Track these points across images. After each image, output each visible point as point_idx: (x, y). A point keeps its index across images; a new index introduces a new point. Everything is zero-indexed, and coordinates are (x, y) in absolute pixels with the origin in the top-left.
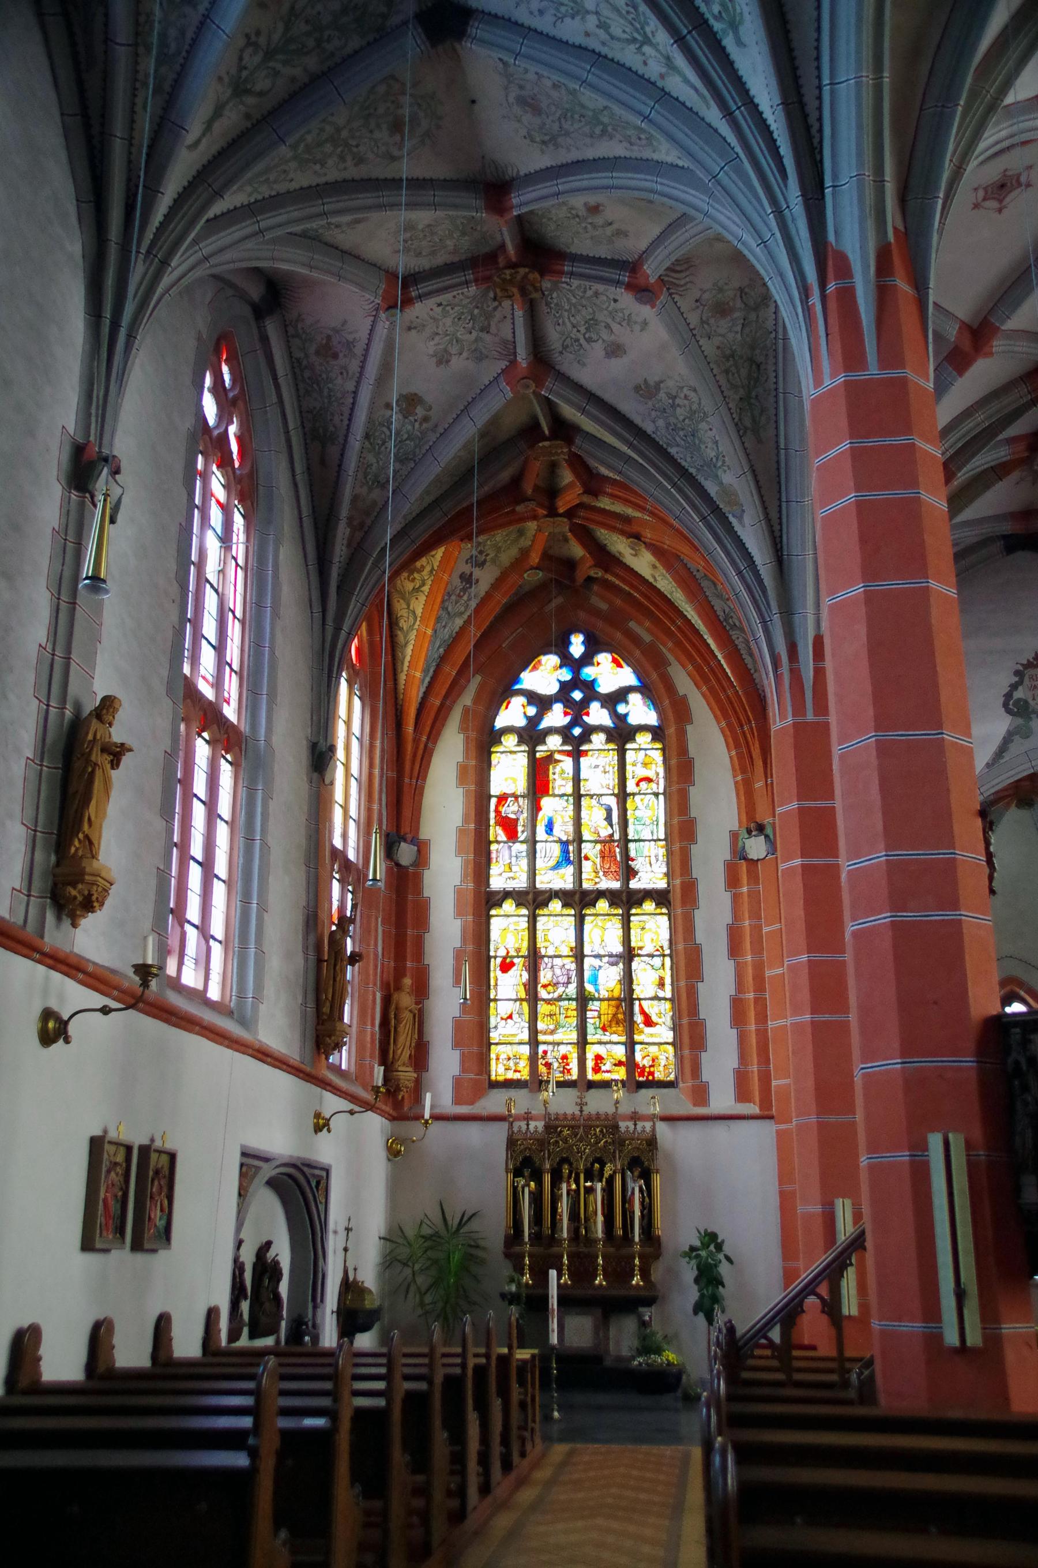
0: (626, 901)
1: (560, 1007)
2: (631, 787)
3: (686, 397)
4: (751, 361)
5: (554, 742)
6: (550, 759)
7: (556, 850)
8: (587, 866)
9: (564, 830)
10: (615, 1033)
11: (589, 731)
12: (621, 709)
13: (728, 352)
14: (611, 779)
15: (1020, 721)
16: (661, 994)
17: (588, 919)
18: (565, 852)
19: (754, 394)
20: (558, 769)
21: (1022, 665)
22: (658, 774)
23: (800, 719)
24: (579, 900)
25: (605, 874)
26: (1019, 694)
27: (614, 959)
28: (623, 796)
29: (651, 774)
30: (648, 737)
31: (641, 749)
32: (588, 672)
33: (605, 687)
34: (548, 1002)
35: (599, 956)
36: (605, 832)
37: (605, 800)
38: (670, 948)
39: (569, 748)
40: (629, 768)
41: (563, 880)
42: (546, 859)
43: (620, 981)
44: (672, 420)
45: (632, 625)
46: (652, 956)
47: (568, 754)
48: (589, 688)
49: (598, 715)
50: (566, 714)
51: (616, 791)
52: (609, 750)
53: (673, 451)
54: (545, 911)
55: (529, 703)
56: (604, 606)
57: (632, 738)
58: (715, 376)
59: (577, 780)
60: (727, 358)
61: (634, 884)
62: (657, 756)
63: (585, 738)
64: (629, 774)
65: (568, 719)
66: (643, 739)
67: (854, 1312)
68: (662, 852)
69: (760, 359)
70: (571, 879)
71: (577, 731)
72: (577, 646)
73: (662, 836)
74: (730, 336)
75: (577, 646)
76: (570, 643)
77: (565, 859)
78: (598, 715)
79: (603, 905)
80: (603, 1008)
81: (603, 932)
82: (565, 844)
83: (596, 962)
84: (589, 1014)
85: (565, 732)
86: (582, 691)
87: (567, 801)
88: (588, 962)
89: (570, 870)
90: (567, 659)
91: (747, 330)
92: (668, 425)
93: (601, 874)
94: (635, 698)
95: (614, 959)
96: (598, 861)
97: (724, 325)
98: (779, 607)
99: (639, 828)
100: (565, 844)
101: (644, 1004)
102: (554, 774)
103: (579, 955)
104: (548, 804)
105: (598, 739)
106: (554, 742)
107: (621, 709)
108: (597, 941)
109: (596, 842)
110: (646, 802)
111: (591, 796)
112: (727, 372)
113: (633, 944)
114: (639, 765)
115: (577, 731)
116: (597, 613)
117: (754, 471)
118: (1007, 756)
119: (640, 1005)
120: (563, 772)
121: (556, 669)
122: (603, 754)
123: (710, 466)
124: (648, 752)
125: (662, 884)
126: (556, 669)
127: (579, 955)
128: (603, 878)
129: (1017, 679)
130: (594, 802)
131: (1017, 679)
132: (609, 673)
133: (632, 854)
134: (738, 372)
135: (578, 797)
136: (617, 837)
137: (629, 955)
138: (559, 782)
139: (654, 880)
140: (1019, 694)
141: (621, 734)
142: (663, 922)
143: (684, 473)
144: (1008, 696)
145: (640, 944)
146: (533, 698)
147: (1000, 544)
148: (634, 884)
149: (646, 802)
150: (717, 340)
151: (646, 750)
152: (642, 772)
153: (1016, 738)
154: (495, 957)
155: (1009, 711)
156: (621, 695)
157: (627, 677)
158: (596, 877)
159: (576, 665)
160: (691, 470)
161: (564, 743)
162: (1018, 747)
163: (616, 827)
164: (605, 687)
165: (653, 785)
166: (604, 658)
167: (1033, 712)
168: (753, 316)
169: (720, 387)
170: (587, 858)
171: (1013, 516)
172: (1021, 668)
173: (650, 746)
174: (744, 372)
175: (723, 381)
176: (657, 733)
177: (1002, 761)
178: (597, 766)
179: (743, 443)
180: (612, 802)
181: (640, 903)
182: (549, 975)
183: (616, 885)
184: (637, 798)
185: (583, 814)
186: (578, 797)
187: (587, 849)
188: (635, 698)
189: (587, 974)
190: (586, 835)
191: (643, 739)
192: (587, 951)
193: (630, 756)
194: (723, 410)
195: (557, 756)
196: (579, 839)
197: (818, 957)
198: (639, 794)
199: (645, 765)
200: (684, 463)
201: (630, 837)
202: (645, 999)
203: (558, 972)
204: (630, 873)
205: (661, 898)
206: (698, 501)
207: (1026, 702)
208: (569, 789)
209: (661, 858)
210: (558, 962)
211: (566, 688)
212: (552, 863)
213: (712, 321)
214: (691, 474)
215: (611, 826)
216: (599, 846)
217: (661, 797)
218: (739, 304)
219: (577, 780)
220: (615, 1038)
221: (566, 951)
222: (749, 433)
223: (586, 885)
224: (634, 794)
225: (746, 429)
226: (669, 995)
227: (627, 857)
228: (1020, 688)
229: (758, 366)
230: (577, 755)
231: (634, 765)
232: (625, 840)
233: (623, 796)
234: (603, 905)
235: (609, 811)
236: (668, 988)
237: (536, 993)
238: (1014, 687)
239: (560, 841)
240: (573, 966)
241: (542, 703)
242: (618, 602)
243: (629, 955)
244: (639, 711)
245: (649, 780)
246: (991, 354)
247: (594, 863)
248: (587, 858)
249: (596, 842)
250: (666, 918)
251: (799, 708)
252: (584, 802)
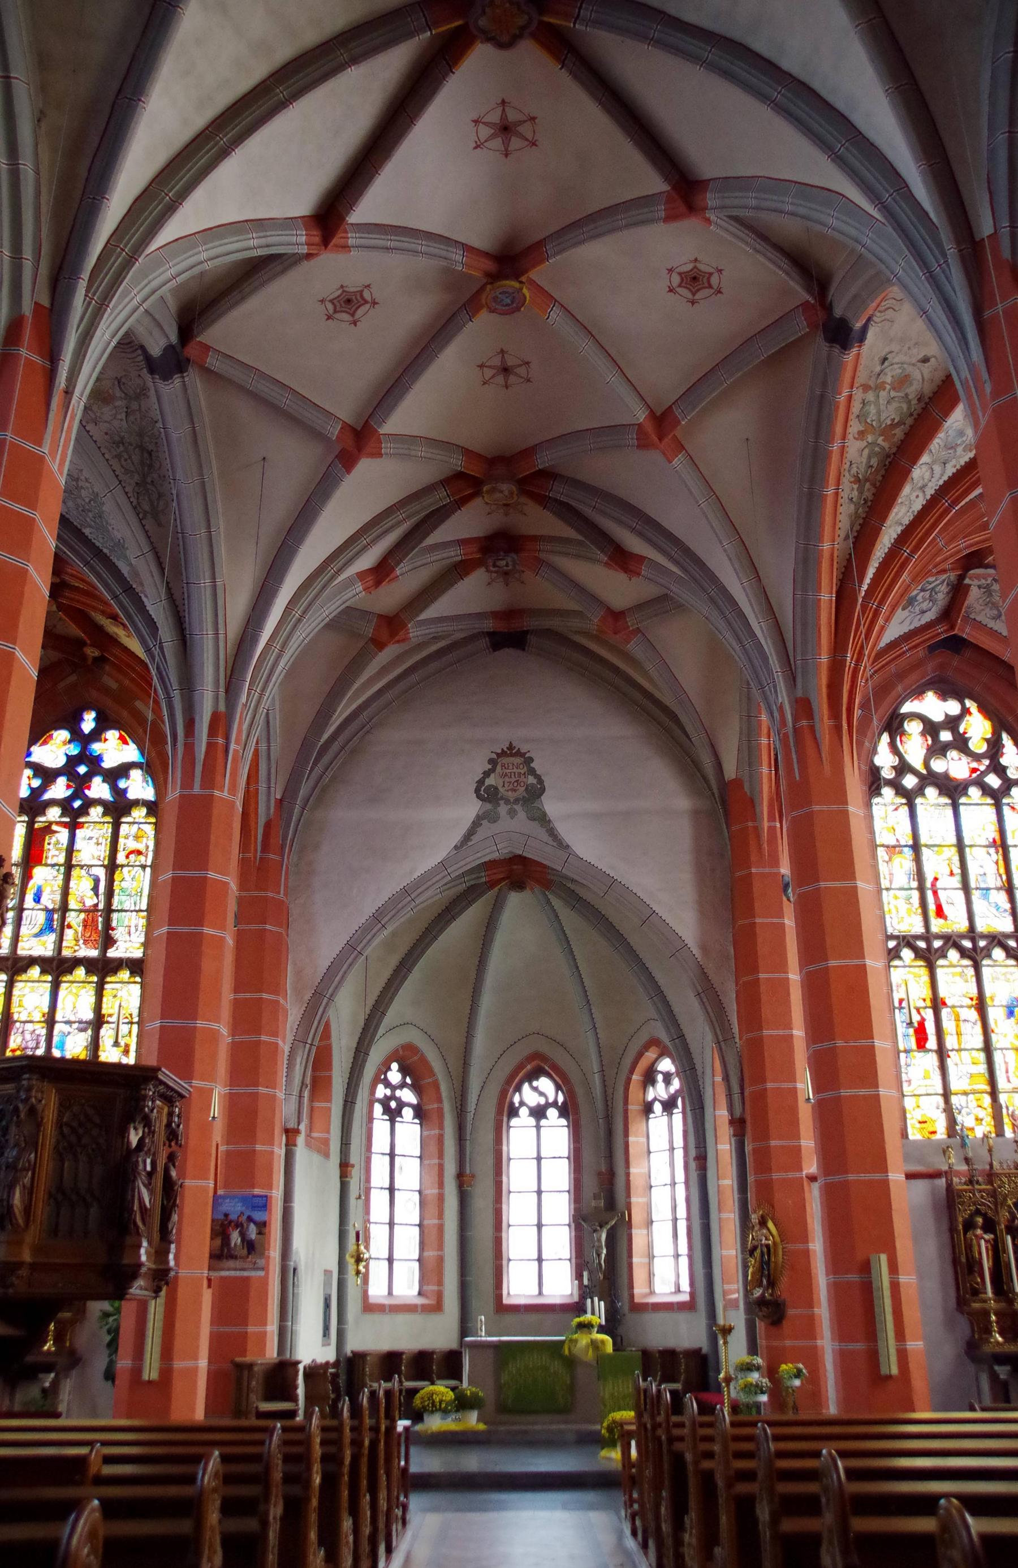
0: (103, 969)
2: (121, 858)
3: (87, 480)
4: (142, 448)
5: (54, 813)
6: (48, 830)
7: (41, 917)
8: (69, 934)
9: (51, 899)
11: (89, 803)
12: (122, 784)
13: (117, 438)
14: (104, 851)
15: (488, 806)
17: (63, 986)
18: (50, 920)
19: (149, 480)
20: (53, 840)
21: (497, 754)
22: (147, 847)
23: (186, 792)
24: (58, 967)
25: (85, 942)
26: (490, 781)
27: (83, 1026)
28: (112, 867)
29: (141, 847)
30: (144, 811)
31: (134, 823)
32: (97, 748)
33: (109, 763)
35: (69, 1023)
36: (90, 902)
37: (95, 871)
39: (67, 820)
40: (121, 841)
41: (44, 947)
42: (31, 927)
43: (86, 1047)
44: (79, 501)
45: (139, 704)
47: (65, 825)
48: (95, 762)
49: (99, 789)
50: (68, 787)
51: (106, 863)
52: (104, 823)
53: (87, 531)
54: (69, 978)
55: (35, 776)
56: (114, 685)
57: (128, 813)
58: (107, 460)
59: (70, 850)
60: (117, 444)
61: (111, 953)
62: (149, 830)
63: (84, 810)
64: (120, 847)
65: (69, 792)
66: (139, 813)
67: (154, 1376)
68: (143, 922)
69: (150, 447)
70: (51, 946)
71: (77, 804)
72: (88, 723)
73: (144, 907)
74: (116, 423)
75: (88, 723)
76: (82, 719)
77: (49, 927)
78: (99, 789)
79: (80, 972)
81: (77, 998)
82: (49, 912)
83: (66, 1028)
85: (65, 805)
86: (87, 766)
87: (58, 870)
88: (58, 1028)
89: (51, 938)
90: (77, 736)
91: (132, 418)
92: (77, 506)
93: (81, 942)
94: (136, 774)
95: (83, 1026)
96: (80, 929)
97: (107, 412)
98: (180, 684)
99: (124, 898)
100: (49, 912)
103: (50, 1021)
104: (40, 874)
105: (96, 812)
106: (54, 813)
107: (122, 784)
108: (69, 1007)
109: (81, 911)
110: (133, 873)
111: (82, 867)
112: (118, 457)
113: (104, 1011)
114: (131, 838)
115: (77, 804)
116: (106, 691)
117: (157, 553)
118: (475, 839)
120: (58, 842)
121: (64, 743)
122: (98, 826)
123: (120, 545)
124: (141, 826)
125: (138, 954)
126: (64, 743)
127: (50, 1021)
128: (83, 946)
129: (490, 767)
130: (83, 872)
131: (490, 767)
132: (115, 749)
133: (114, 924)
134: (130, 457)
135: (69, 867)
136: (101, 906)
137: (99, 1021)
138: (53, 852)
139: (131, 949)
140: (490, 781)
141: (119, 808)
142: (136, 990)
143: (98, 553)
144: (481, 782)
145: (110, 1012)
146: (39, 770)
147: (484, 643)
148: (111, 953)
149: (133, 873)
150: (104, 427)
152: (132, 845)
153: (485, 822)
155: (479, 796)
156: (123, 770)
157: (131, 753)
158: (77, 946)
159: (84, 740)
160: (105, 551)
161: (62, 815)
162: (486, 830)
163: (102, 897)
164: (109, 763)
165: (142, 858)
166: (112, 735)
167: (502, 798)
168: (134, 405)
169: (114, 471)
170: (69, 927)
171: (495, 615)
172: (495, 756)
173: (143, 821)
174: (136, 458)
175: (117, 467)
176: (152, 808)
177: (470, 844)
178: (90, 838)
179: (144, 526)
180: (101, 873)
181: (115, 971)
182: (19, 1039)
183: (94, 953)
184: (126, 869)
185: (72, 884)
186: (69, 867)
187: (72, 918)
188: (136, 774)
189: (56, 1039)
190: (73, 904)
191: (139, 813)
192: (58, 1017)
193: (124, 829)
194: (118, 492)
195: (54, 827)
196: (64, 908)
197: (169, 1023)
198: (128, 865)
199: (137, 838)
200: (98, 544)
201: (113, 908)
203: (28, 1037)
204: (108, 941)
205: (136, 967)
206: (110, 581)
207: (496, 788)
208: (61, 859)
209: (140, 928)
210: (29, 1027)
211: (72, 761)
212: (36, 930)
213: (95, 408)
214: (105, 555)
215: (97, 895)
216: (83, 916)
217: (148, 870)
218: (118, 394)
219: (70, 850)
221: (38, 1016)
222: (149, 516)
223: (66, 953)
224: (122, 866)
225: (145, 513)
227: (108, 926)
228: (492, 775)
229: (150, 453)
230: (73, 827)
231: (127, 837)
232: (109, 910)
233: (112, 867)
234: (80, 972)
235: (97, 881)
238: (487, 774)
239: (46, 909)
240: (44, 1032)
241: (47, 775)
242: (127, 682)
243: (99, 1021)
244: (139, 787)
245: (139, 853)
246: (380, 455)
247: (76, 932)
248: (69, 927)
249: (81, 911)
250: (138, 986)
251: (188, 781)
252: (75, 872)
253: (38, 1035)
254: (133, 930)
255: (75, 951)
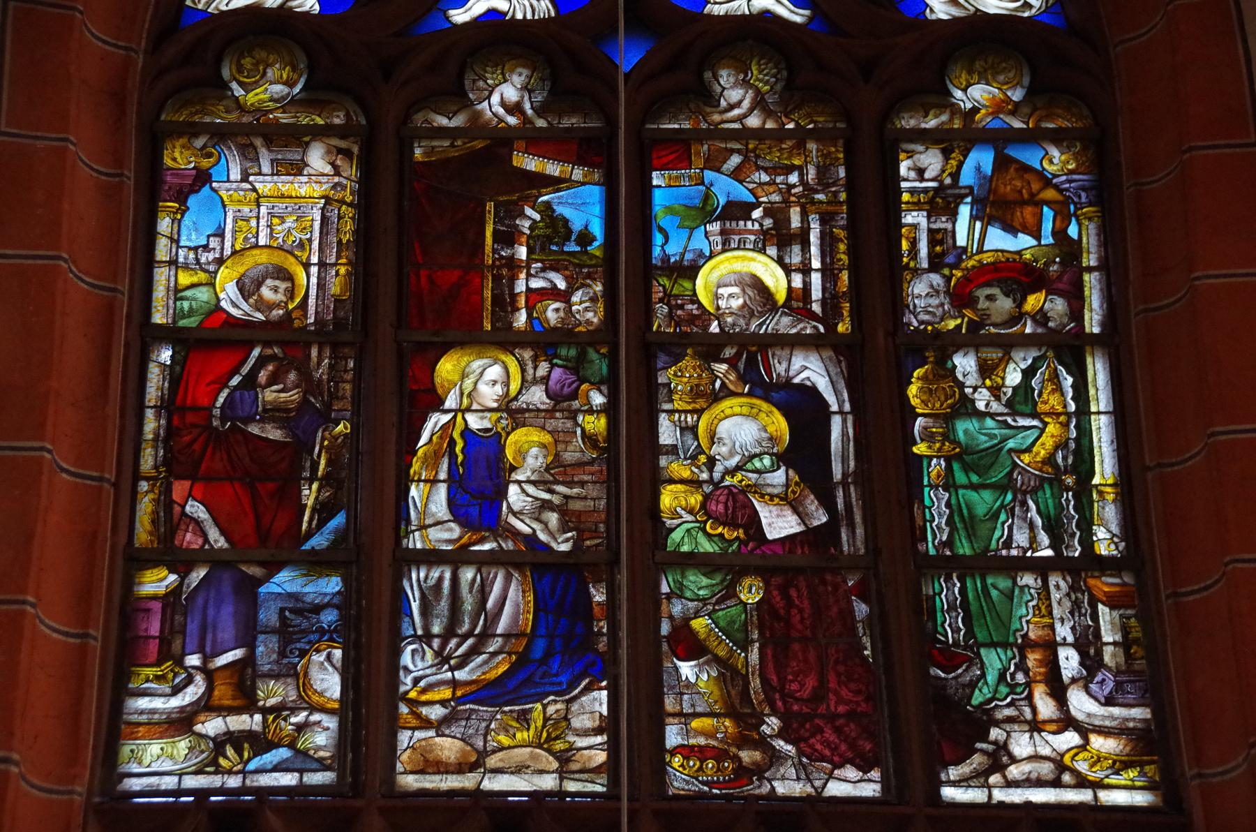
22: (1069, 250)
52: (800, 137)
87: (577, 368)
93: (772, 724)
99: (982, 501)
102: (507, 238)
104: (477, 382)
110: (1013, 377)
111: (710, 350)
114: (965, 211)
122: (773, 157)
136: (852, 541)
139: (1082, 767)
151: (999, 140)
193: (919, 168)
198: (972, 338)
199: (996, 208)
231: (942, 202)
247: (730, 675)
254: (1069, 661)
255: (744, 773)
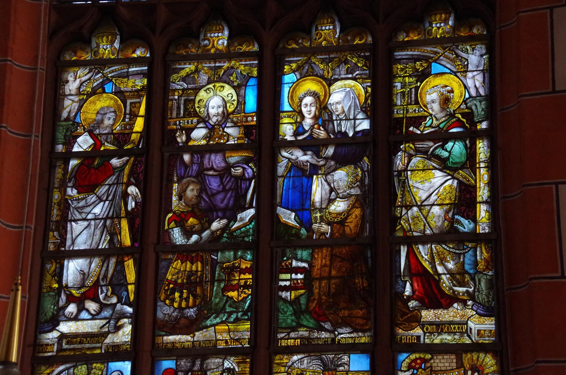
1: (214, 263)
10: (345, 323)
16: (466, 225)
34: (185, 253)
38: (490, 115)
46: (441, 137)
80: (318, 263)
84: (285, 279)
101: (423, 251)
108: (309, 109)
113: (398, 113)
119: (411, 254)
142: (475, 58)
154: (71, 155)
182: (191, 192)
202: (424, 240)
203: (214, 184)
210: (217, 160)
220: (345, 335)
226: (483, 228)
236: (482, 212)
237: (164, 236)
250: (481, 49)
253: (242, 177)
